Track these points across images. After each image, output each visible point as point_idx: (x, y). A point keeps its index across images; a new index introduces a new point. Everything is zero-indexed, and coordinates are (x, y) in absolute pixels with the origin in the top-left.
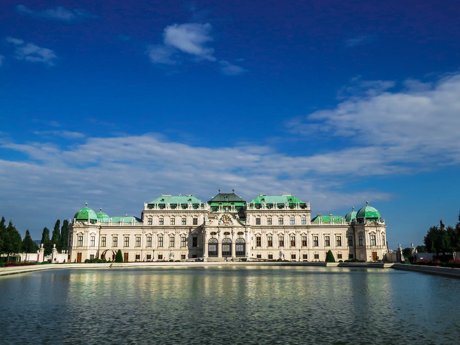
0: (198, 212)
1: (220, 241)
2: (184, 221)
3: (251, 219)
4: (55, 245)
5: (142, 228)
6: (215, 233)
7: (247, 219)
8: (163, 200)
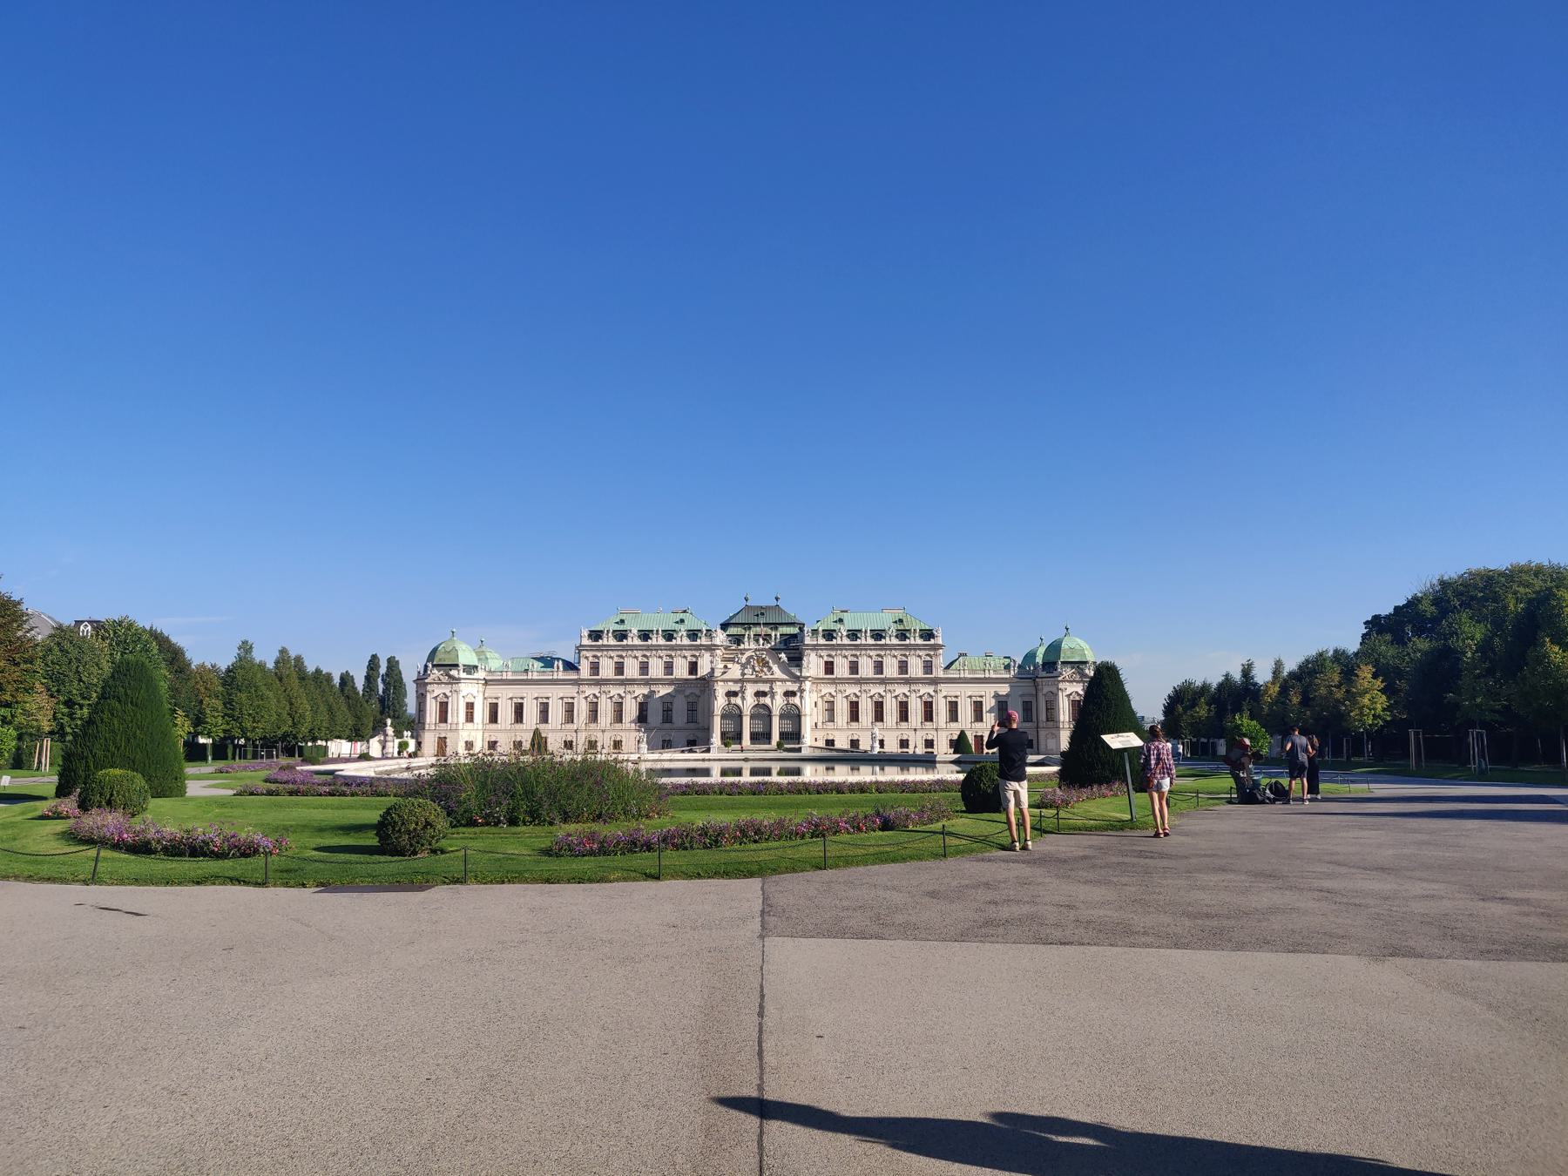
0: (698, 648)
1: (747, 711)
2: (669, 668)
3: (813, 665)
4: (389, 721)
5: (577, 683)
6: (735, 694)
7: (805, 663)
8: (622, 621)
